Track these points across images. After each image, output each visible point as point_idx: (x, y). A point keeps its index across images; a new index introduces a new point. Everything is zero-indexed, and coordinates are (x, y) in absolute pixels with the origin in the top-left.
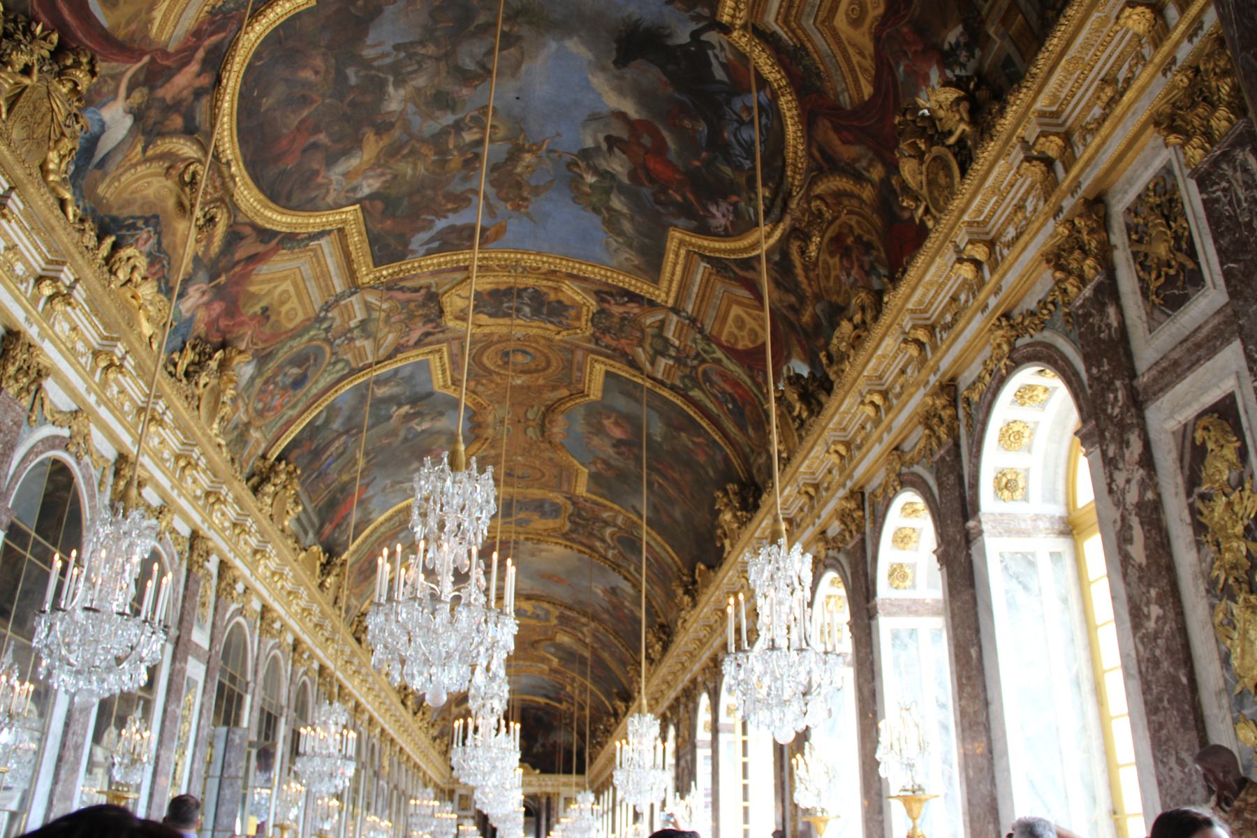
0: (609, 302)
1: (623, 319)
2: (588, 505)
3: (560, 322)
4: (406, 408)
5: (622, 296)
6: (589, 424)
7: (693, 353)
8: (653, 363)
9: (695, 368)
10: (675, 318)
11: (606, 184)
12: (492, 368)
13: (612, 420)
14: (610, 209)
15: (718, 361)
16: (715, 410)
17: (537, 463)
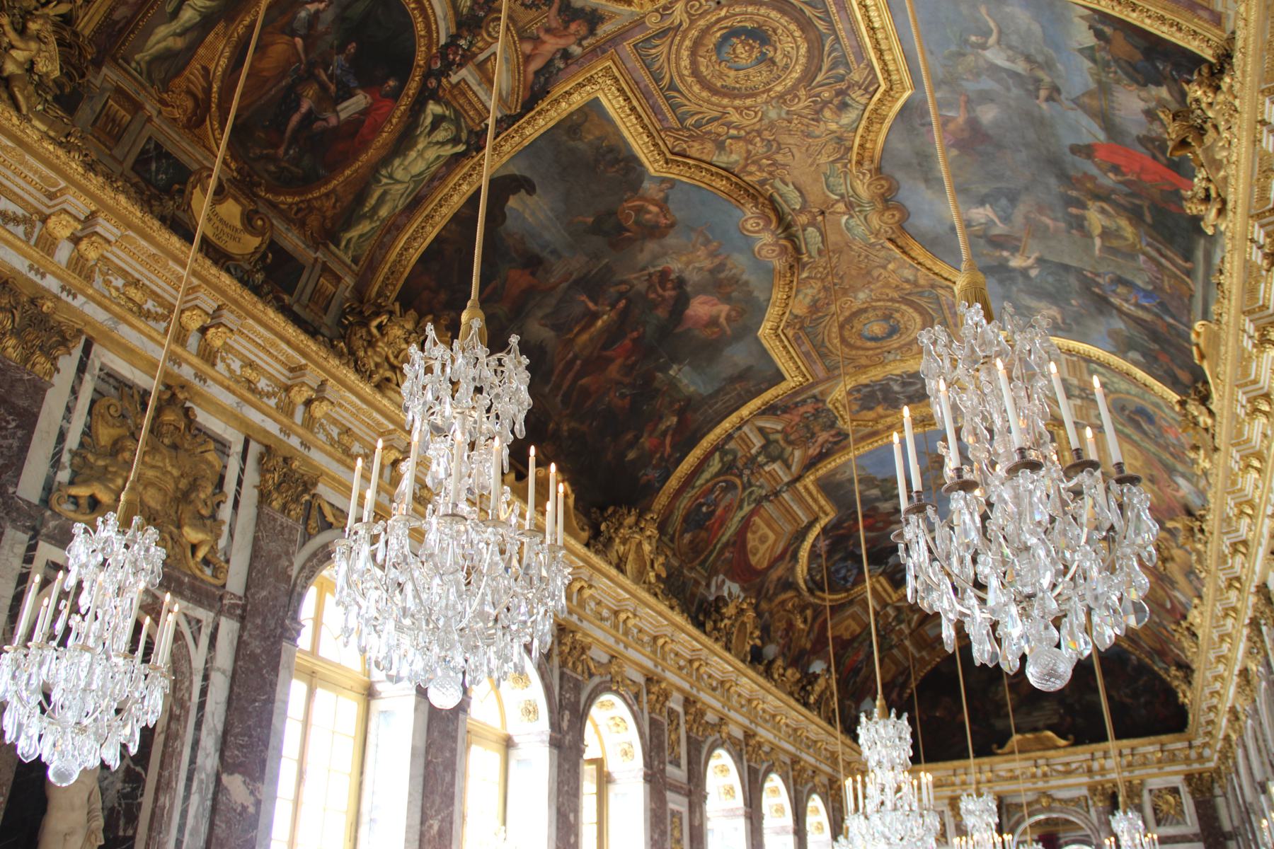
0: (833, 436)
1: (813, 435)
2: (552, 44)
3: (859, 391)
4: (1016, 262)
5: (828, 450)
6: (734, 281)
7: (753, 481)
8: (761, 430)
9: (740, 476)
10: (786, 479)
11: (887, 496)
12: (904, 307)
13: (722, 320)
14: (877, 486)
15: (740, 507)
16: (698, 483)
17: (734, 117)
